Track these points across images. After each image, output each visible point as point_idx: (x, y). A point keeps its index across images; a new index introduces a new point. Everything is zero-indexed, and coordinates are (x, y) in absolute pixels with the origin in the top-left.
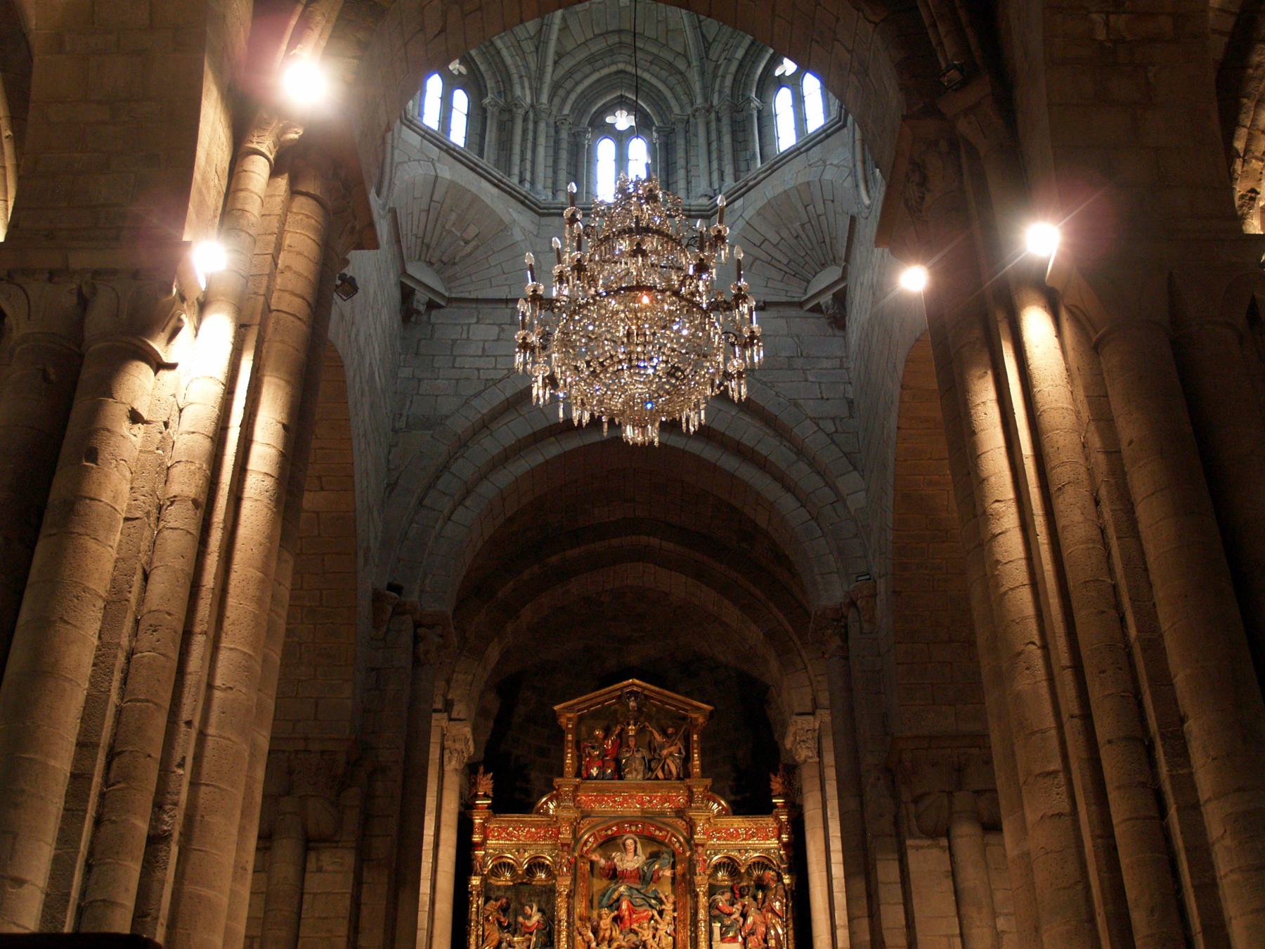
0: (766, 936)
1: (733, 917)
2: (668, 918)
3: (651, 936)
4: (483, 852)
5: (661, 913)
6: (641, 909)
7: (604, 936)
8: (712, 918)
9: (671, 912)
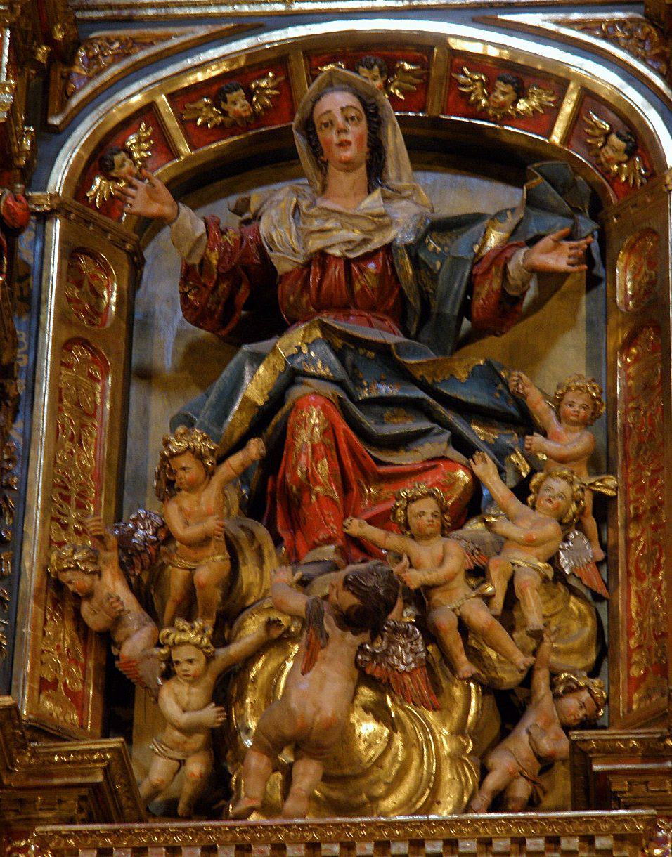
6: (406, 459)
7: (191, 590)
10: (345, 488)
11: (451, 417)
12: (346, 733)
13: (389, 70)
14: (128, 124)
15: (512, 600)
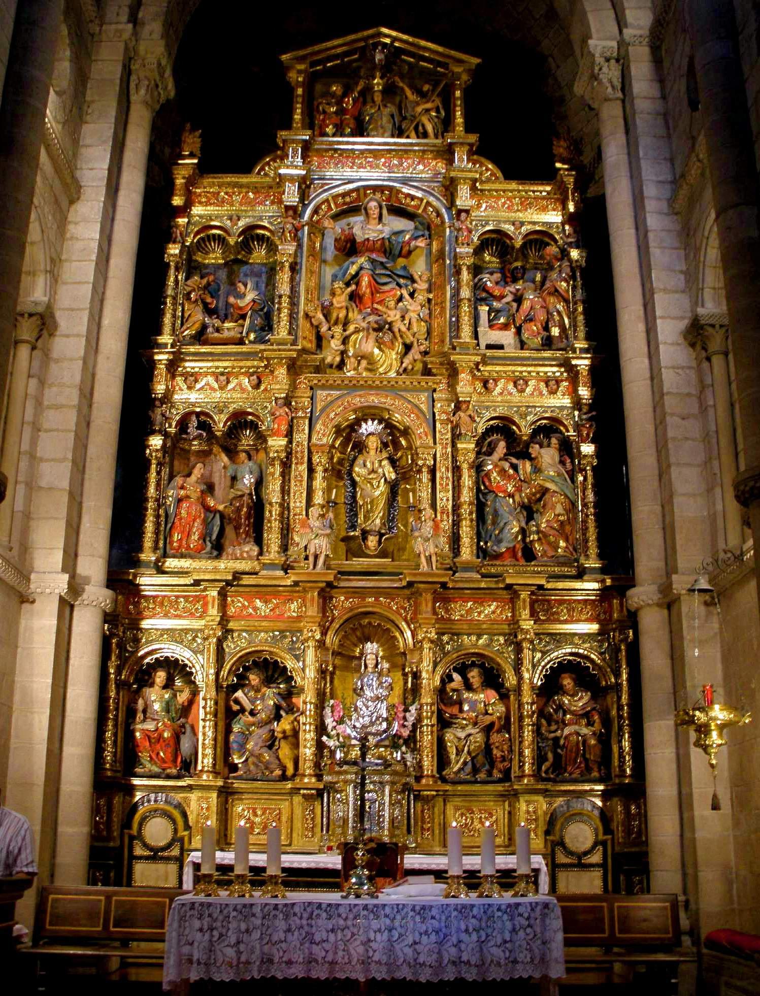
0: (547, 323)
1: (505, 300)
2: (421, 297)
3: (398, 316)
6: (386, 288)
7: (338, 318)
8: (477, 301)
10: (372, 294)
11: (395, 277)
12: (372, 353)
13: (382, 192)
14: (323, 203)
15: (410, 323)
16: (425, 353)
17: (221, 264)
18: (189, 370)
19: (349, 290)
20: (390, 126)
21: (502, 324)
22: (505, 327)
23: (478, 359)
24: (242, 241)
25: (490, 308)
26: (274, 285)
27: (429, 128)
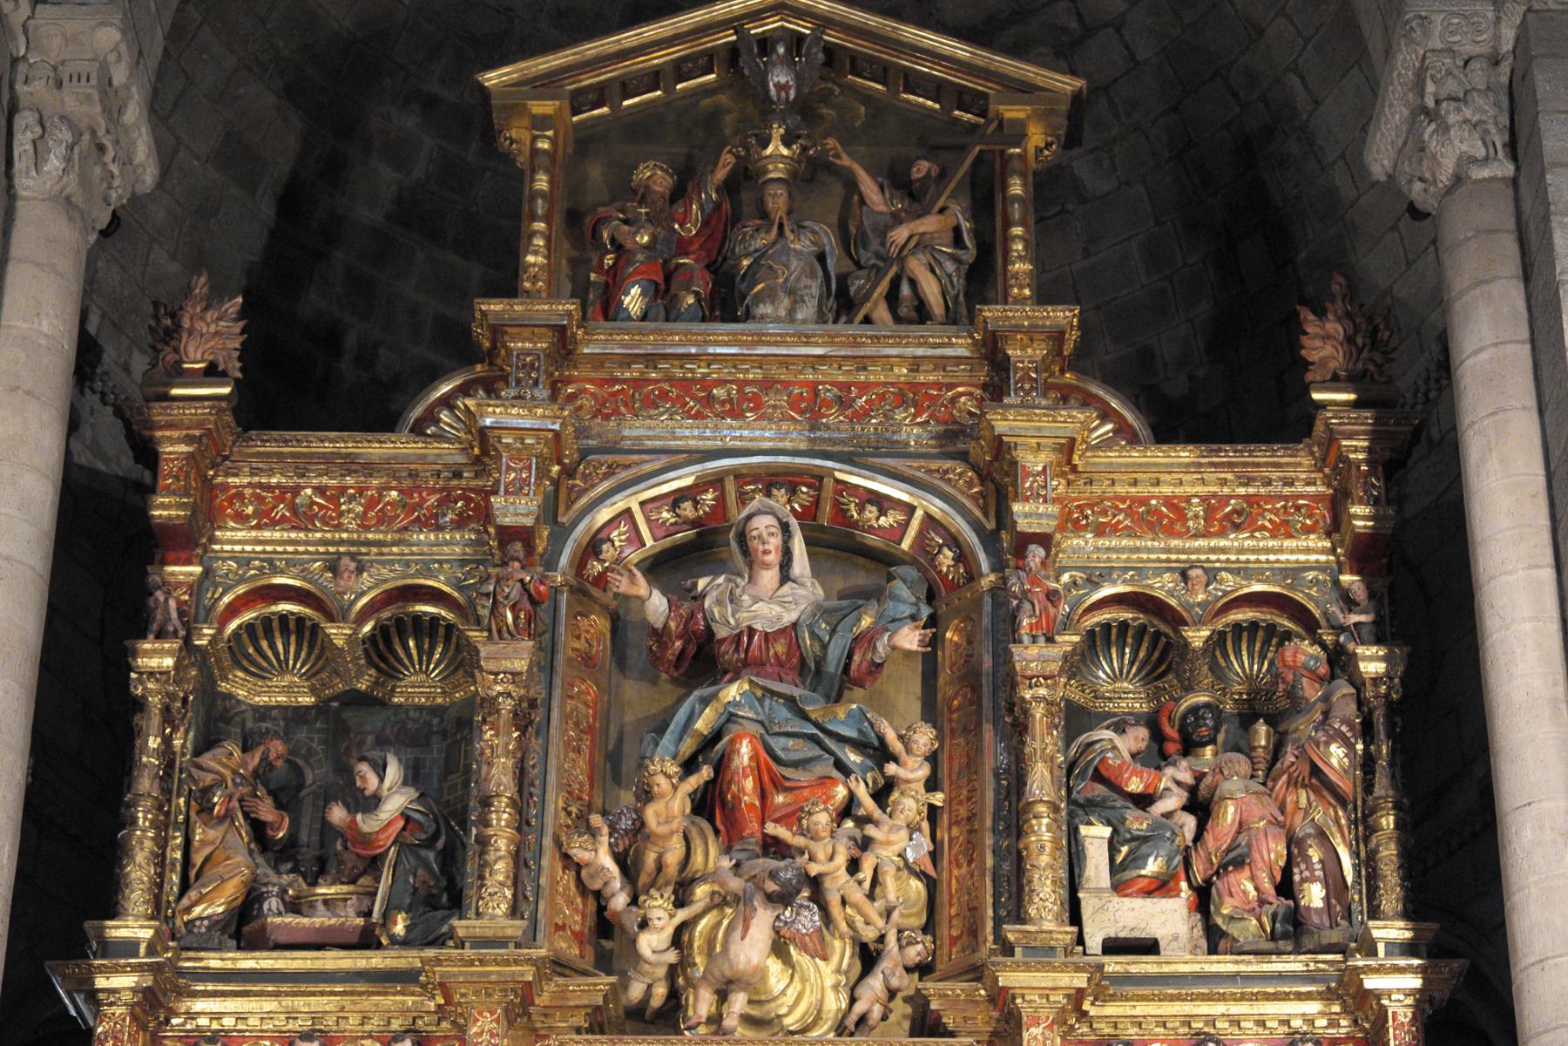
0: (1287, 871)
2: (910, 804)
3: (841, 860)
4: (198, 569)
5: (882, 795)
8: (1077, 810)
9: (920, 787)
10: (763, 796)
12: (762, 972)
13: (793, 490)
15: (875, 882)
16: (923, 969)
17: (307, 708)
18: (203, 1021)
19: (694, 781)
20: (815, 287)
21: (1155, 877)
22: (1161, 887)
23: (1080, 981)
24: (372, 638)
25: (1115, 832)
26: (468, 769)
27: (931, 290)
